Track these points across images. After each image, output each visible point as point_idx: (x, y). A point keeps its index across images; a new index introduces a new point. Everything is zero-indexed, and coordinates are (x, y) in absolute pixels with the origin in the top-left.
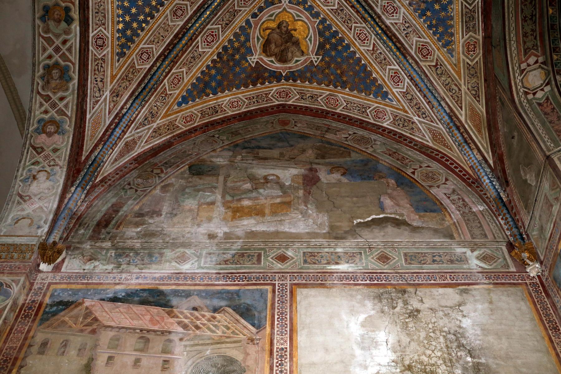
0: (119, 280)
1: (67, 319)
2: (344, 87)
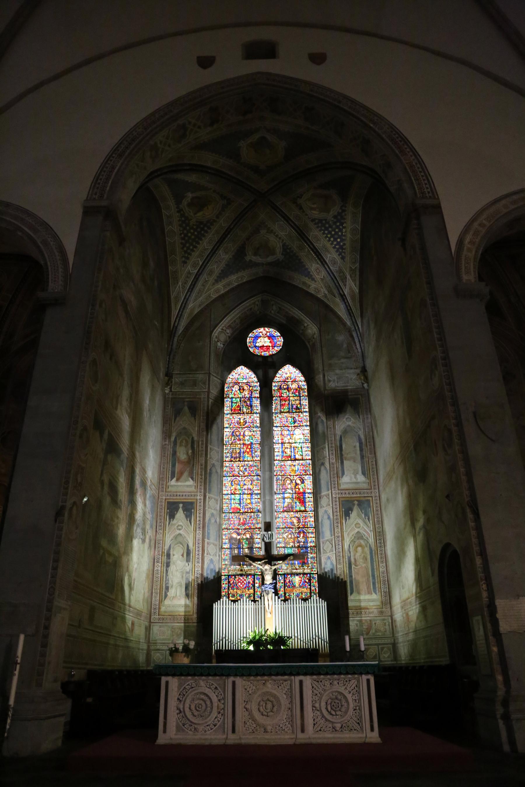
2: (183, 239)
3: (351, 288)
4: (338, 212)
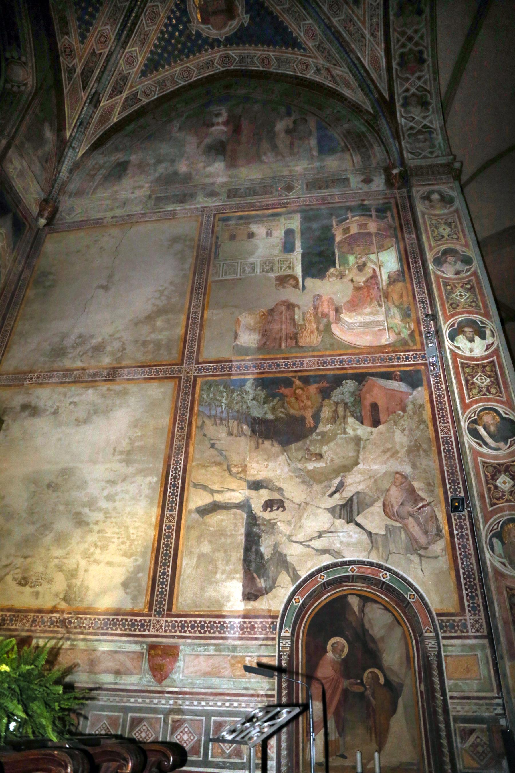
3: (112, 108)
4: (207, 38)
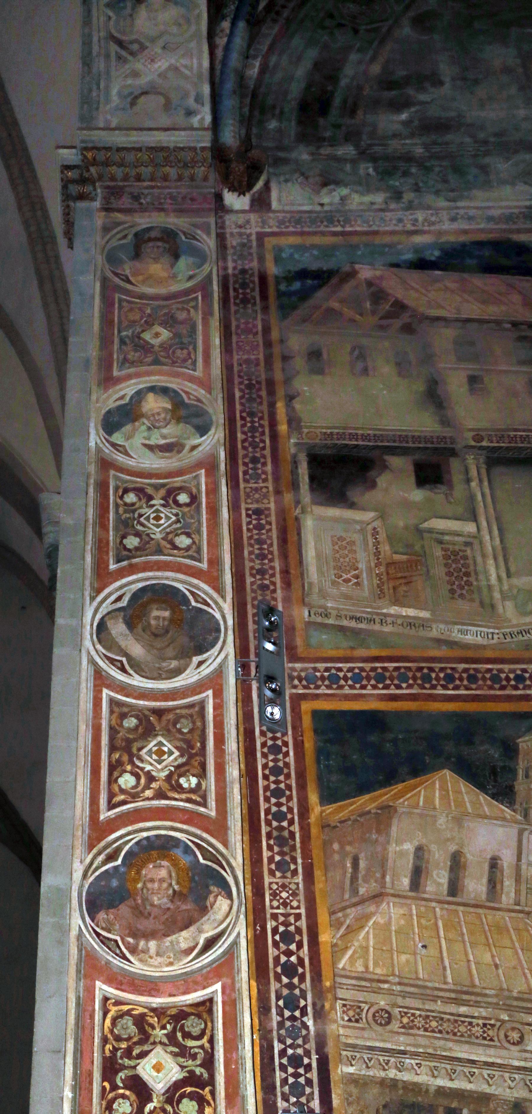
0: (414, 225)
1: (335, 305)
